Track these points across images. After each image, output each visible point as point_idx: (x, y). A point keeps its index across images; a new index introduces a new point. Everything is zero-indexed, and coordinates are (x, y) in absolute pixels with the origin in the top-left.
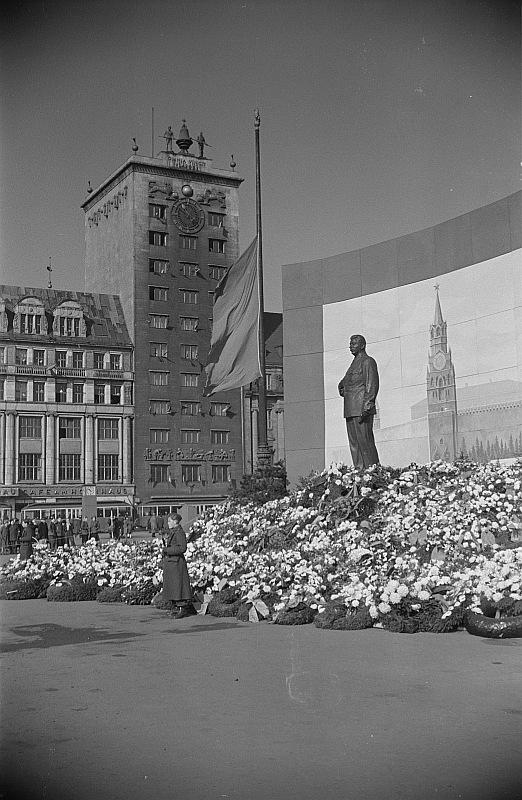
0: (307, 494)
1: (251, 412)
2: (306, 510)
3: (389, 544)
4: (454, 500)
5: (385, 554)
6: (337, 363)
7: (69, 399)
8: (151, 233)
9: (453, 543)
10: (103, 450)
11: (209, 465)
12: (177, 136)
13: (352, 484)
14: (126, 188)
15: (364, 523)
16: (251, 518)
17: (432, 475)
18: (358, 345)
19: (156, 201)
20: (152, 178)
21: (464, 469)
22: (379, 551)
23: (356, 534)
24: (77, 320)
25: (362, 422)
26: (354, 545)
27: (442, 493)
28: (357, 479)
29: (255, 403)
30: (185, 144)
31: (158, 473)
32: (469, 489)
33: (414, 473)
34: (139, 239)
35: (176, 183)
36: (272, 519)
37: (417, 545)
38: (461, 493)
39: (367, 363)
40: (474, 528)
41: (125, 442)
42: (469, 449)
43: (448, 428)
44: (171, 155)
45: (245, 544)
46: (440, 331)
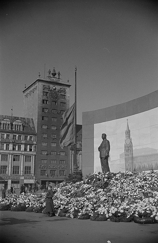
0: (88, 180)
1: (72, 155)
2: (88, 185)
3: (112, 196)
4: (132, 183)
5: (111, 199)
6: (98, 142)
7: (17, 149)
8: (43, 100)
9: (131, 196)
10: (26, 165)
11: (59, 170)
12: (52, 72)
13: (102, 177)
14: (36, 87)
15: (105, 190)
16: (72, 187)
17: (125, 175)
18: (104, 136)
19: (45, 91)
20: (44, 84)
21: (135, 174)
22: (109, 198)
23: (103, 193)
24: (20, 125)
25: (105, 159)
26: (102, 196)
27: (128, 181)
28: (103, 176)
29: (73, 152)
30: (54, 74)
31: (43, 172)
32: (136, 180)
33: (120, 175)
34: (40, 102)
35: (51, 86)
36: (78, 188)
37: (121, 196)
38: (134, 181)
39: (106, 142)
40: (137, 191)
41: (33, 161)
42: (137, 168)
43: (130, 161)
45: (70, 195)
46: (128, 133)
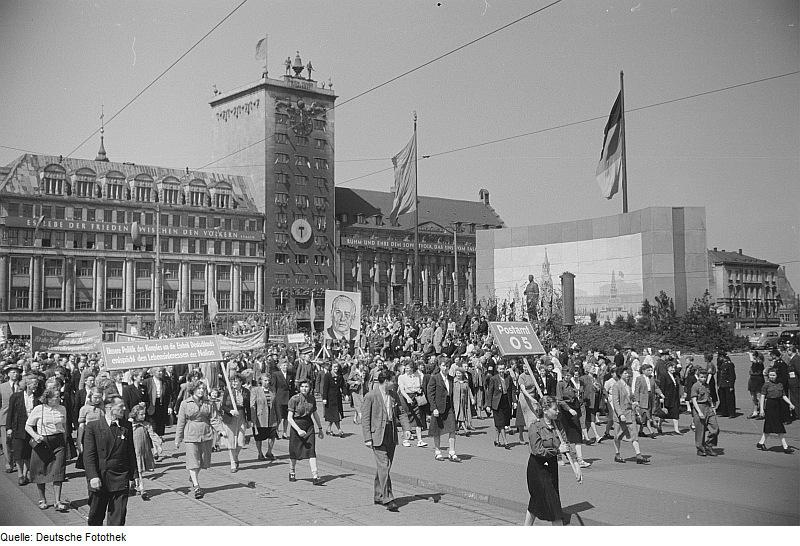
12: (293, 64)
20: (277, 94)
30: (298, 70)
35: (294, 98)
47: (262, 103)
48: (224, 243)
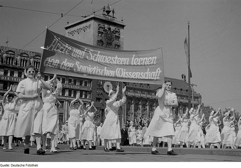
35: (106, 26)
44: (105, 16)
47: (92, 26)
48: (73, 91)
